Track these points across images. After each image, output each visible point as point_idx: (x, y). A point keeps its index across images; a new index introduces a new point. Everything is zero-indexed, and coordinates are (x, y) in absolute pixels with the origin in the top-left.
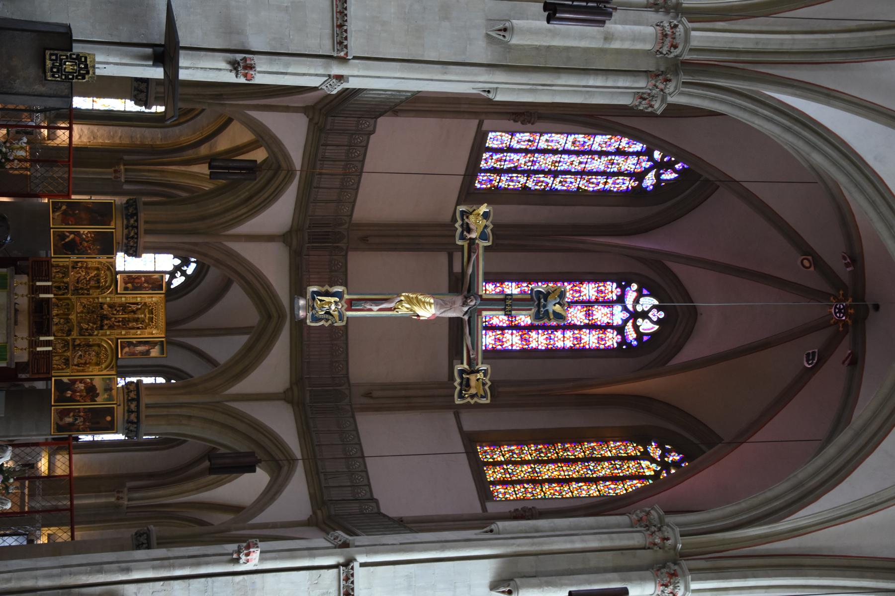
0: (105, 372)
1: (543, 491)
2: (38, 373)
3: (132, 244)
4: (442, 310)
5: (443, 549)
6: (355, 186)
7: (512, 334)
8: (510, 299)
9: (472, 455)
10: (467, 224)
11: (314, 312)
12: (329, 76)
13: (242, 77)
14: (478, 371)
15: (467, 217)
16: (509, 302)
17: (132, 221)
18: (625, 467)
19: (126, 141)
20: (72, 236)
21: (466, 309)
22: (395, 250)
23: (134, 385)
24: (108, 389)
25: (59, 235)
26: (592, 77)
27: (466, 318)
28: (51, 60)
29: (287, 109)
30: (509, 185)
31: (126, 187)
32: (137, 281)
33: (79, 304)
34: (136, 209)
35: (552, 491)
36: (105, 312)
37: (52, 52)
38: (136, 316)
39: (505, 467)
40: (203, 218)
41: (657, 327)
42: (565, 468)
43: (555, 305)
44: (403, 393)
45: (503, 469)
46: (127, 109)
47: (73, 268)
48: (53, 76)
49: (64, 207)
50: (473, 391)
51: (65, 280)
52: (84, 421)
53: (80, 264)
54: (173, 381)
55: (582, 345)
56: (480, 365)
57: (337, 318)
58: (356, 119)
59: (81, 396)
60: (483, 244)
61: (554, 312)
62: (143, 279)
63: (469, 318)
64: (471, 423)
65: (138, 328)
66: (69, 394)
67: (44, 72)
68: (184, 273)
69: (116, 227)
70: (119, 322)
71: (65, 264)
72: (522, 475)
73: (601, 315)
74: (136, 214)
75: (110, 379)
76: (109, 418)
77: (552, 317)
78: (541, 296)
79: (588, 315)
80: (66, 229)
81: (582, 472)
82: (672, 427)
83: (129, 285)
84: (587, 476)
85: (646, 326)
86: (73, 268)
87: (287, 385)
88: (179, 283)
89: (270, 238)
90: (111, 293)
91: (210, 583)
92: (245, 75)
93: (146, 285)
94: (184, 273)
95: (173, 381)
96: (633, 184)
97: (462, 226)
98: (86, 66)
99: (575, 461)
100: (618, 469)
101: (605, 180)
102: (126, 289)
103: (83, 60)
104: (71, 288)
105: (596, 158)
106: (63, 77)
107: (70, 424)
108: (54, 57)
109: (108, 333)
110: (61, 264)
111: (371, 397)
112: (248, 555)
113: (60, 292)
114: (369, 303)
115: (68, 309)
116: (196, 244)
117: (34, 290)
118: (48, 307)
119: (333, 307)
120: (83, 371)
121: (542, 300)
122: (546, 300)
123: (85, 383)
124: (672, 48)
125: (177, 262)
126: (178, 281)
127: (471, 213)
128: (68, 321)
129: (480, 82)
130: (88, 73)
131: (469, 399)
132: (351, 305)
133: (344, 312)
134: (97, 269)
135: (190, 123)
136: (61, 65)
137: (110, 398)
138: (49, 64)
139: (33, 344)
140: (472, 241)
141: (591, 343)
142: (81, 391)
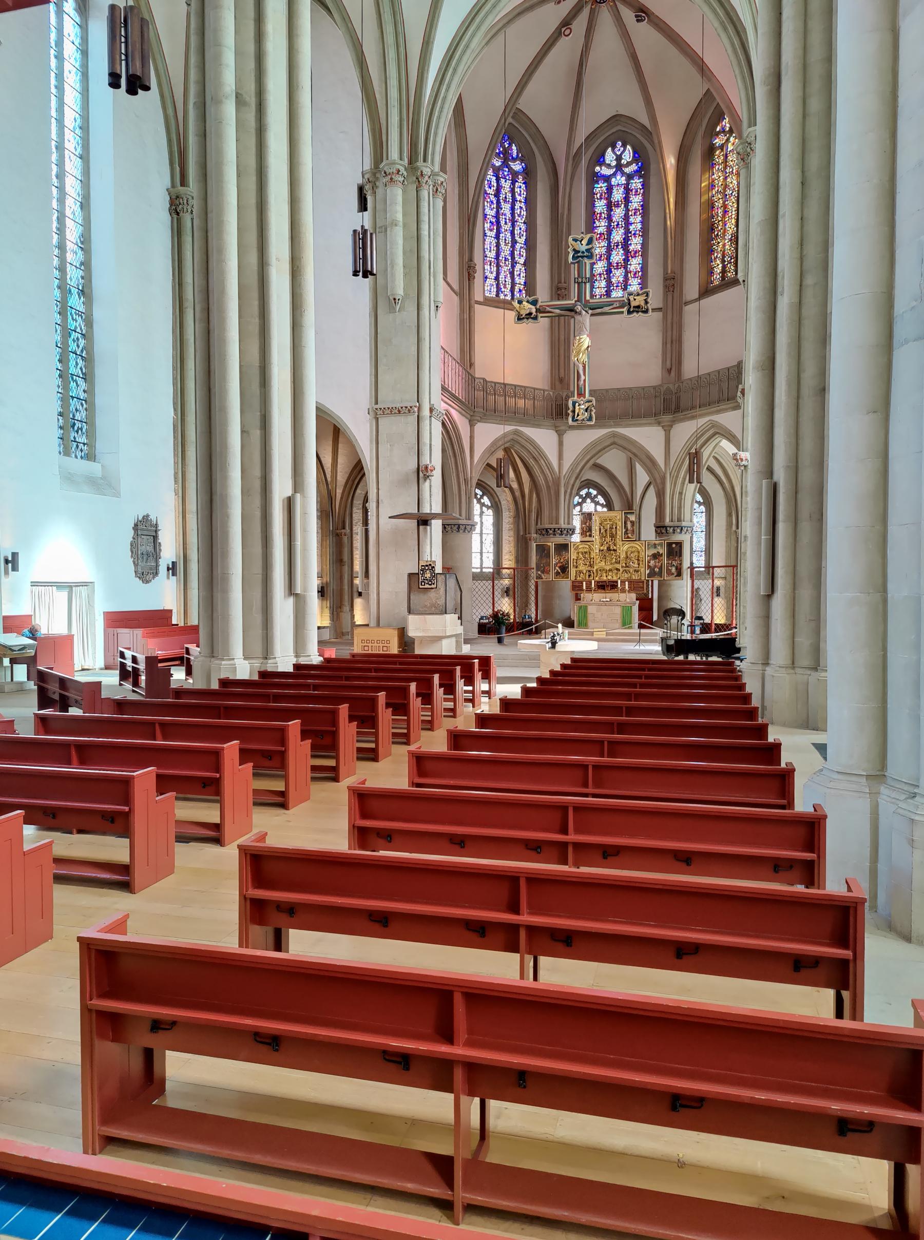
0: (643, 548)
2: (643, 588)
3: (565, 532)
6: (523, 389)
7: (630, 265)
17: (551, 532)
19: (512, 533)
20: (557, 568)
24: (655, 546)
26: (422, 232)
29: (472, 437)
32: (585, 529)
33: (600, 564)
36: (606, 548)
38: (608, 529)
40: (548, 487)
41: (628, 147)
46: (492, 533)
47: (577, 567)
48: (434, 584)
49: (539, 572)
51: (584, 572)
53: (575, 564)
55: (640, 208)
58: (476, 392)
65: (616, 528)
67: (432, 588)
68: (596, 496)
69: (552, 542)
71: (574, 572)
73: (618, 195)
74: (547, 529)
75: (648, 545)
76: (674, 546)
79: (618, 206)
85: (627, 156)
86: (577, 567)
87: (660, 428)
88: (602, 499)
89: (561, 444)
93: (588, 524)
94: (596, 496)
102: (590, 536)
104: (589, 568)
107: (676, 569)
109: (618, 546)
110: (574, 575)
113: (592, 575)
115: (603, 570)
116: (565, 492)
117: (589, 589)
123: (650, 560)
124: (400, 173)
125: (589, 500)
126: (601, 499)
128: (610, 570)
134: (578, 553)
135: (498, 494)
137: (661, 545)
139: (623, 591)
141: (638, 201)
142: (655, 562)
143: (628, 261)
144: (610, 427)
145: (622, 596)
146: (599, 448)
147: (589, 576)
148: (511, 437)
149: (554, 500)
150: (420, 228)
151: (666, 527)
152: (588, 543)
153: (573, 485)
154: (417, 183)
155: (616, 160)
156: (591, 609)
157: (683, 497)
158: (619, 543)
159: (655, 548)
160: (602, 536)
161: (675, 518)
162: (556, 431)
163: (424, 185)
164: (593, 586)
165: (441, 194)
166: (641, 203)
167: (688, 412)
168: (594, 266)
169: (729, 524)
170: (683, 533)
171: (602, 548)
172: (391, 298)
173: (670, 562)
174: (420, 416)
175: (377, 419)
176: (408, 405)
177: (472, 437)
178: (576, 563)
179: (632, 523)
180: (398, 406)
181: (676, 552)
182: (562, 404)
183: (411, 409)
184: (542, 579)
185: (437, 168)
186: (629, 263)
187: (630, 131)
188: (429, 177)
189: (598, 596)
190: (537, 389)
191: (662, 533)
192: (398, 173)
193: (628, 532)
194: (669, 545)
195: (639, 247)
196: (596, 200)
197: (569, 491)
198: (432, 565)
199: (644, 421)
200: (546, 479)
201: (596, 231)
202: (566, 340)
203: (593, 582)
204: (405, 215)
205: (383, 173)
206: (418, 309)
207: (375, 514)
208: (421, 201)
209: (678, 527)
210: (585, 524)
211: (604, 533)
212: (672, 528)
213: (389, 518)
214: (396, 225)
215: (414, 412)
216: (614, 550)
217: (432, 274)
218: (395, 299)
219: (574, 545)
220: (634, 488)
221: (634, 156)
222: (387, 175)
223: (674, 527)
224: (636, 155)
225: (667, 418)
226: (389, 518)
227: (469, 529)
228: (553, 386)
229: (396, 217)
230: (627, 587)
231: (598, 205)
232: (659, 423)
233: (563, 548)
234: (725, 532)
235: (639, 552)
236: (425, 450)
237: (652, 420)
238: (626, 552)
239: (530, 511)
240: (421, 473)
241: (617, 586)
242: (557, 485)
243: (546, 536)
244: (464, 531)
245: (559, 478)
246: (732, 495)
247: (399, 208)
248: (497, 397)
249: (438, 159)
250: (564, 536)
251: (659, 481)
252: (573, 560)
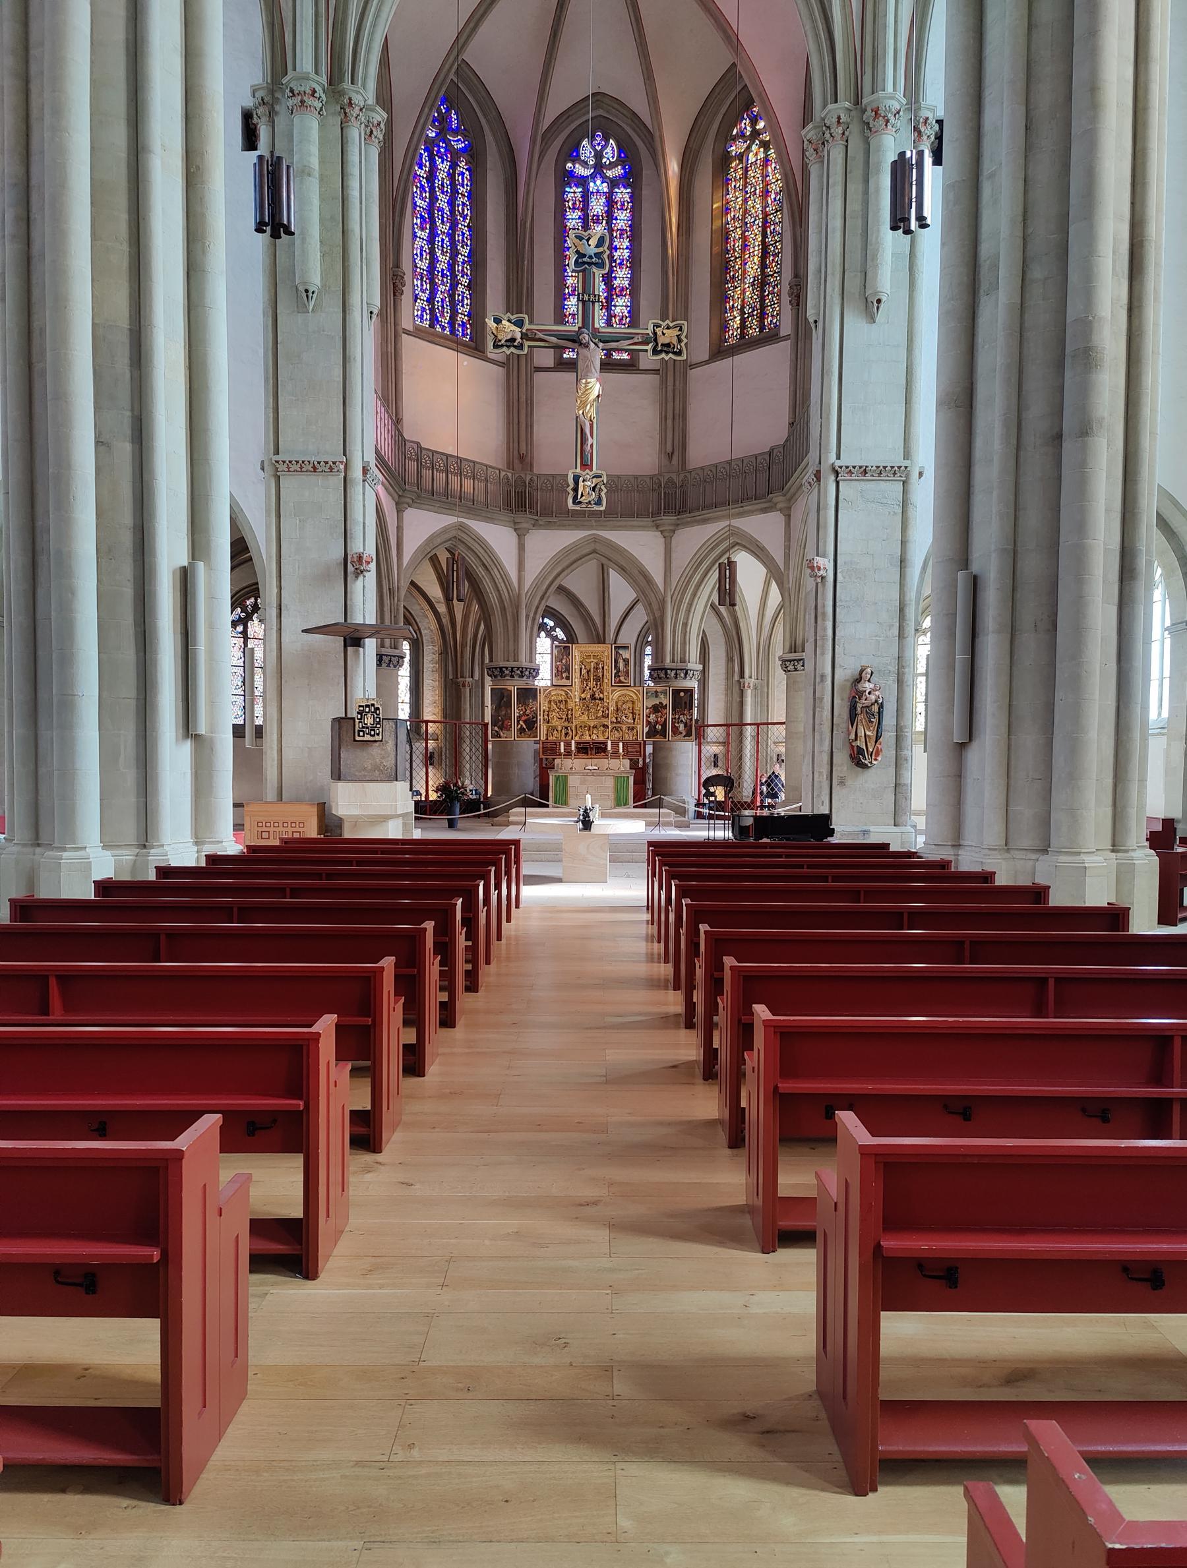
0: (641, 697)
1: (773, 275)
2: (640, 752)
3: (527, 673)
4: (593, 370)
5: (830, 372)
6: (471, 464)
7: (615, 306)
8: (583, 295)
9: (733, 351)
10: (506, 341)
11: (592, 502)
12: (364, 481)
13: (369, 566)
14: (655, 333)
15: (500, 341)
16: (586, 297)
18: (754, 181)
19: (436, 675)
20: (521, 722)
21: (592, 345)
22: (532, 426)
23: (653, 673)
24: (656, 694)
25: (521, 733)
27: (601, 345)
28: (364, 736)
29: (399, 528)
30: (467, 305)
31: (477, 676)
32: (560, 669)
34: (496, 668)
35: (774, 264)
37: (357, 734)
38: (592, 670)
39: (746, 316)
40: (503, 609)
42: (752, 250)
43: (590, 245)
44: (669, 422)
45: (748, 317)
47: (548, 722)
48: (378, 734)
49: (496, 728)
50: (675, 341)
51: (559, 729)
52: (684, 714)
53: (546, 717)
54: (650, 639)
55: (628, 229)
56: (649, 332)
57: (600, 479)
58: (407, 461)
59: (661, 717)
60: (527, 326)
61: (597, 246)
62: (558, 663)
63: (601, 341)
64: (701, 350)
65: (603, 668)
66: (659, 727)
67: (375, 741)
68: (553, 629)
69: (513, 686)
70: (597, 684)
71: (545, 729)
72: (755, 297)
73: (597, 206)
74: (501, 668)
76: (682, 694)
77: (601, 249)
78: (580, 260)
80: (515, 728)
81: (756, 231)
82: (715, 126)
83: (564, 675)
84: (760, 225)
85: (610, 153)
86: (548, 722)
88: (561, 633)
89: (521, 548)
90: (571, 691)
91: (841, 604)
92: (368, 563)
93: (564, 661)
94: (553, 629)
95: (650, 639)
96: (464, 164)
97: (508, 347)
98: (367, 706)
99: (744, 238)
100: (756, 189)
101: (460, 196)
102: (568, 678)
103: (362, 709)
104: (566, 724)
105: (438, 205)
106: (378, 726)
108: (361, 734)
110: (545, 732)
111: (672, 453)
112: (819, 569)
113: (570, 732)
114: (585, 446)
115: (585, 726)
116: (527, 616)
117: (568, 753)
118: (583, 743)
119: (588, 483)
120: (639, 715)
121: (584, 260)
122: (584, 256)
123: (650, 714)
125: (543, 634)
126: (560, 634)
127: (496, 336)
128: (595, 727)
129: (362, 321)
130: (373, 705)
131: (683, 344)
132: (586, 465)
133: (593, 473)
134: (550, 702)
135: (418, 620)
136: (367, 728)
137: (665, 693)
138: (367, 738)
139: (615, 755)
140: (524, 336)
141: (626, 218)
142: (657, 717)
143: (612, 300)
144: (591, 528)
145: (614, 763)
146: (574, 557)
147: (566, 734)
148: (453, 533)
149: (511, 627)
150: (348, 186)
151: (666, 670)
152: (565, 689)
153: (537, 608)
154: (343, 116)
155: (595, 156)
156: (573, 781)
157: (688, 630)
158: (607, 688)
159: (657, 696)
160: (584, 680)
161: (678, 657)
162: (515, 530)
163: (353, 119)
164: (573, 748)
165: (377, 141)
166: (630, 222)
167: (698, 513)
168: (566, 303)
169: (729, 673)
170: (688, 678)
171: (583, 696)
172: (302, 289)
173: (677, 717)
174: (348, 478)
175: (278, 479)
176: (330, 459)
177: (399, 528)
178: (548, 715)
179: (626, 661)
180: (313, 459)
181: (685, 703)
182: (525, 491)
183: (333, 466)
184: (500, 737)
185: (371, 100)
186: (613, 303)
187: (615, 119)
188: (361, 110)
189: (578, 763)
190: (490, 467)
191: (660, 678)
192: (313, 95)
193: (620, 674)
194: (676, 693)
195: (626, 283)
196: (568, 210)
197: (531, 615)
198: (376, 706)
199: (636, 522)
200: (501, 597)
201: (567, 253)
202: (529, 402)
203: (573, 742)
204: (322, 162)
205: (288, 91)
206: (344, 311)
207: (275, 628)
208: (349, 144)
209: (681, 670)
210: (561, 661)
211: (586, 675)
212: (674, 672)
213: (303, 631)
214: (309, 175)
215: (338, 471)
216: (600, 699)
217: (364, 260)
218: (307, 291)
219: (544, 691)
220: (607, 619)
221: (619, 156)
222: (294, 95)
223: (676, 670)
224: (623, 155)
225: (668, 520)
226: (303, 631)
227: (395, 662)
228: (510, 465)
229: (309, 162)
230: (621, 751)
231: (570, 217)
232: (657, 527)
233: (529, 694)
234: (724, 683)
235: (633, 703)
236: (356, 531)
237: (647, 521)
238: (617, 703)
239: (463, 645)
240: (350, 566)
241: (606, 748)
242: (517, 608)
243: (499, 678)
244: (388, 665)
245: (519, 596)
246: (734, 633)
247: (314, 149)
248: (435, 472)
249: (372, 84)
250: (525, 678)
251: (655, 607)
252: (544, 711)
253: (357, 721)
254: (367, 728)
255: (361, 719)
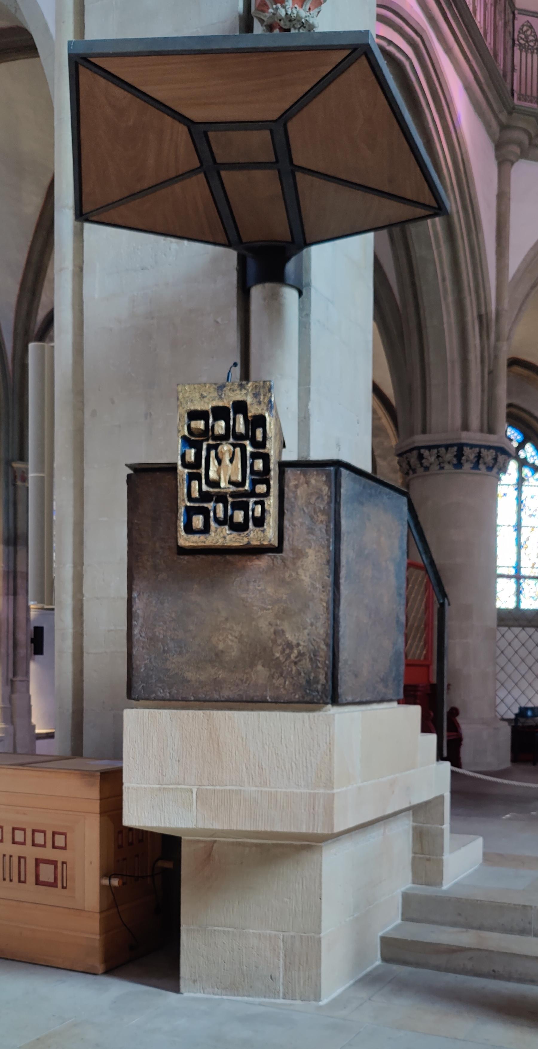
28: (206, 530)
48: (260, 522)
103: (200, 424)
106: (261, 488)
130: (241, 407)
136: (221, 498)
198: (253, 411)
253: (183, 472)
254: (221, 498)
255: (197, 464)
